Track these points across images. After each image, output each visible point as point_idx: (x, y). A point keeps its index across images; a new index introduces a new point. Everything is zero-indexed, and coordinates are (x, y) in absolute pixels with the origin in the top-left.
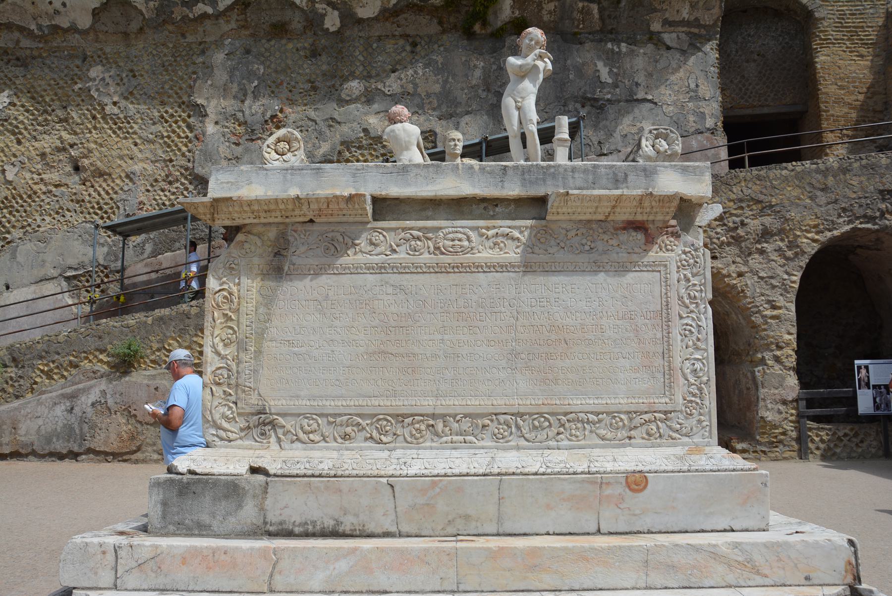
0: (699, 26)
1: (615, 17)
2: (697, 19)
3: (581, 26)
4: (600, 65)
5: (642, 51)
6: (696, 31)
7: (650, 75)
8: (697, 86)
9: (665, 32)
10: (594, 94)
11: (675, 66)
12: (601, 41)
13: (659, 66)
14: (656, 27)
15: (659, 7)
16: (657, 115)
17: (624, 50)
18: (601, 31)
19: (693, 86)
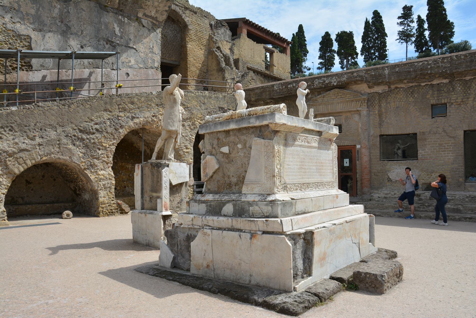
0: (157, 21)
1: (125, 5)
2: (156, 17)
3: (109, 3)
4: (116, 25)
5: (133, 24)
6: (155, 22)
7: (135, 37)
8: (153, 47)
9: (143, 19)
10: (112, 39)
11: (145, 35)
12: (116, 13)
13: (140, 33)
14: (140, 15)
15: (144, 7)
16: (137, 56)
17: (126, 21)
18: (117, 9)
19: (151, 47)
